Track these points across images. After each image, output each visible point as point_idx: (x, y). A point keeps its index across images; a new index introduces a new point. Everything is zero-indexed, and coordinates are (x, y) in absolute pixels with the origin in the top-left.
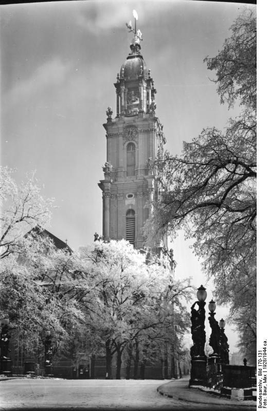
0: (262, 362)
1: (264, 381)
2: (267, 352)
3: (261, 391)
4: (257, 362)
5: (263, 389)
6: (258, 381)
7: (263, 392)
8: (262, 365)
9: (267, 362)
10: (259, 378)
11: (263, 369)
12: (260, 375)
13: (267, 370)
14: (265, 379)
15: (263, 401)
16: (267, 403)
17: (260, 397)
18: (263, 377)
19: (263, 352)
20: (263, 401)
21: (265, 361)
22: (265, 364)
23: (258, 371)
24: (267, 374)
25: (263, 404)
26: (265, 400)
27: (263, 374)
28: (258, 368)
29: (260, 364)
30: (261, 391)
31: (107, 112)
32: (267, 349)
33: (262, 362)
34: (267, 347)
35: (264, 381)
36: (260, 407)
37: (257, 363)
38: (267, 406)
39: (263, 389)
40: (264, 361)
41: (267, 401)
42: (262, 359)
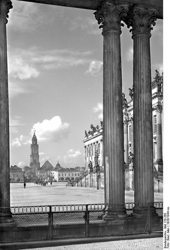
0: (166, 220)
1: (168, 232)
2: (169, 214)
3: (166, 238)
4: (164, 220)
5: (167, 237)
6: (164, 232)
7: (167, 238)
8: (167, 222)
9: (169, 220)
10: (164, 230)
11: (167, 225)
12: (165, 228)
13: (169, 225)
14: (168, 230)
15: (167, 244)
16: (169, 245)
17: (165, 241)
18: (167, 229)
19: (167, 214)
20: (167, 244)
21: (168, 219)
22: (168, 221)
23: (164, 225)
25: (167, 246)
26: (168, 243)
27: (167, 227)
28: (164, 223)
29: (165, 222)
30: (166, 238)
31: (40, 123)
32: (169, 213)
33: (166, 220)
34: (169, 211)
35: (168, 232)
36: (165, 248)
37: (164, 223)
38: (169, 247)
39: (167, 237)
40: (168, 219)
41: (169, 244)
42: (166, 218)
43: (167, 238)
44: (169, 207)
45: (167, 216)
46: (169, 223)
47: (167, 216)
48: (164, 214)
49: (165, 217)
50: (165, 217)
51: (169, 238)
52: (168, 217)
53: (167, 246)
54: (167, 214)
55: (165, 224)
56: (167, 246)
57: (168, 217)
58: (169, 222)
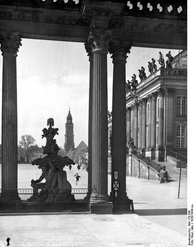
0: (191, 218)
1: (192, 229)
2: (193, 212)
3: (190, 235)
5: (191, 234)
7: (191, 235)
8: (191, 219)
11: (191, 222)
12: (189, 225)
13: (193, 222)
14: (192, 228)
15: (191, 241)
17: (189, 238)
18: (191, 226)
19: (191, 212)
20: (191, 241)
21: (192, 217)
22: (192, 219)
24: (193, 225)
25: (191, 243)
27: (191, 225)
29: (189, 219)
30: (190, 235)
32: (193, 210)
33: (191, 218)
34: (193, 208)
35: (192, 229)
36: (189, 245)
38: (193, 244)
39: (191, 234)
42: (190, 216)
43: (191, 235)
44: (193, 205)
45: (191, 213)
46: (193, 221)
47: (191, 213)
48: (188, 212)
49: (189, 215)
50: (189, 215)
51: (193, 235)
52: (192, 215)
53: (191, 243)
54: (191, 212)
55: (189, 221)
56: (191, 243)
57: (192, 215)
58: (193, 219)
